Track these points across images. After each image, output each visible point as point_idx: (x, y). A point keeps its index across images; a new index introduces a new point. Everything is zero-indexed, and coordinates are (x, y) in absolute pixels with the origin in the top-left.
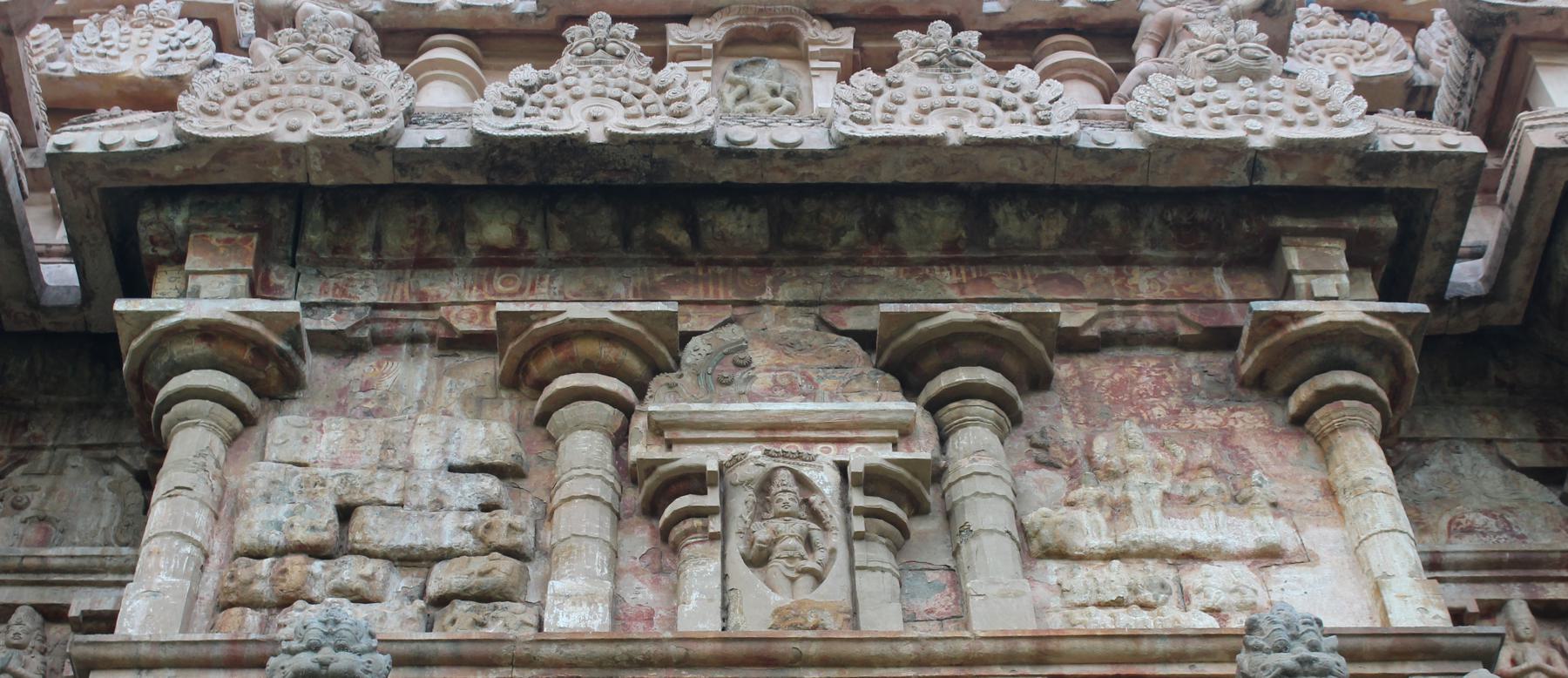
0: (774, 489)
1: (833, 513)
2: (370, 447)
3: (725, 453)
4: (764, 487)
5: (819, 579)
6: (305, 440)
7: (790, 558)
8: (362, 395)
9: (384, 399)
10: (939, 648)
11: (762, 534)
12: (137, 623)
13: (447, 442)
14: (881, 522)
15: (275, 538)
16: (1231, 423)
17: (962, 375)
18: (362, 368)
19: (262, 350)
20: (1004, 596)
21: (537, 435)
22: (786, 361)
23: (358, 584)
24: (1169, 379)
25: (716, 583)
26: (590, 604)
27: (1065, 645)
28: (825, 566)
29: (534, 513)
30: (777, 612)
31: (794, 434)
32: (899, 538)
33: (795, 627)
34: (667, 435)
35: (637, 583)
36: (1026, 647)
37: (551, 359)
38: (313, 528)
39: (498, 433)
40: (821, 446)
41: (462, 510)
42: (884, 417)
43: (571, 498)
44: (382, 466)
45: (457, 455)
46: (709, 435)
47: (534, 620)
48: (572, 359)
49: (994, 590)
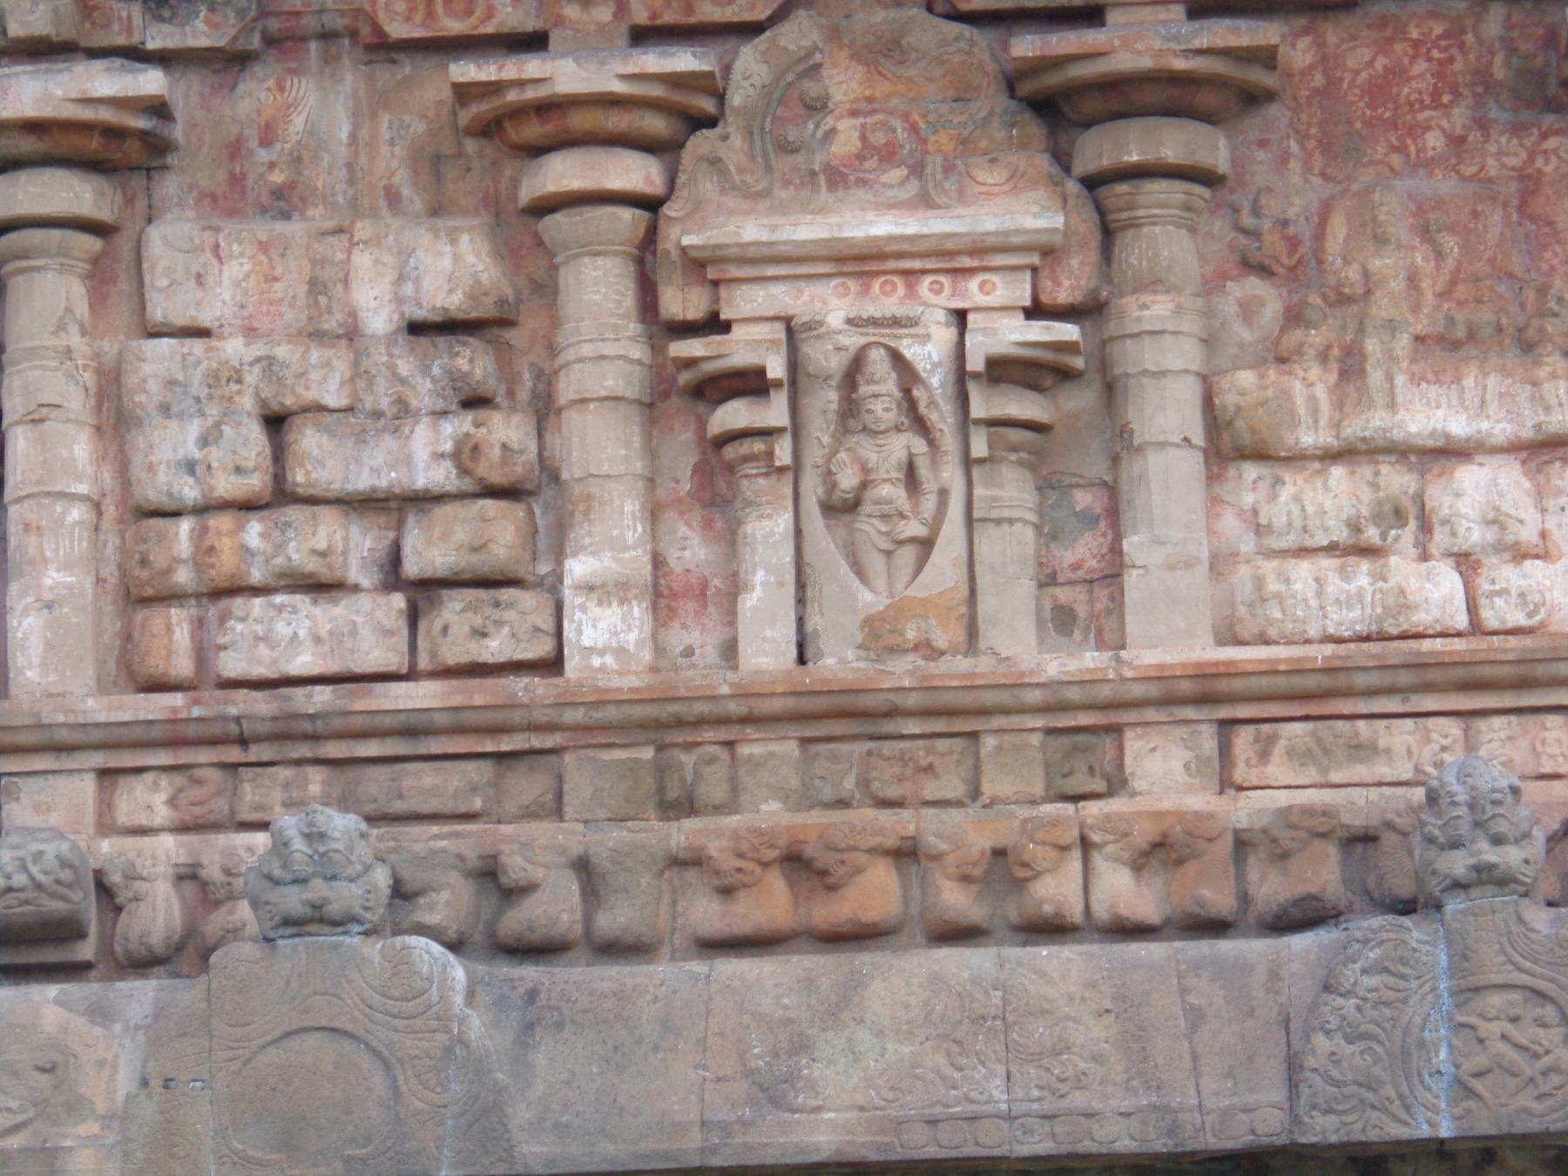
1: (943, 418)
2: (292, 282)
5: (926, 545)
6: (200, 279)
7: (885, 517)
8: (263, 155)
9: (296, 160)
10: (1073, 694)
11: (848, 480)
12: (36, 660)
14: (1015, 435)
15: (189, 492)
16: (1539, 162)
18: (255, 93)
19: (113, 133)
20: (1171, 568)
22: (882, 88)
23: (312, 565)
24: (1458, 66)
25: (787, 556)
27: (1238, 685)
34: (712, 273)
35: (683, 530)
38: (238, 470)
39: (471, 259)
40: (928, 279)
41: (434, 413)
42: (1016, 240)
43: (584, 401)
44: (318, 336)
45: (419, 305)
46: (771, 271)
47: (547, 624)
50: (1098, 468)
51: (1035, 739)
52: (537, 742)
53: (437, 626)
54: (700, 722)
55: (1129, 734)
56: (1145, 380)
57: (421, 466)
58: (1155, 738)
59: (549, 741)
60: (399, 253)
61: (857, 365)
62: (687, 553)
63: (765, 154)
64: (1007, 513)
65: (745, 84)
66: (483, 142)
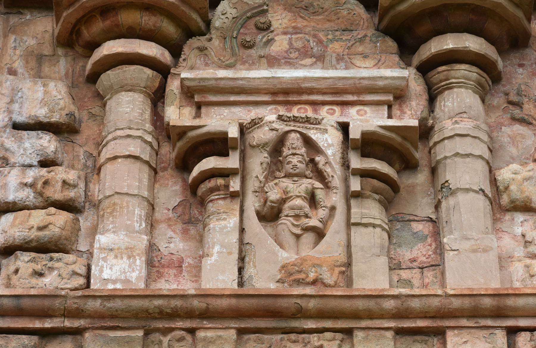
0: (286, 151)
1: (334, 172)
3: (246, 115)
4: (277, 148)
5: (319, 234)
7: (297, 217)
10: (415, 304)
11: (274, 195)
13: (12, 101)
14: (375, 182)
17: (449, 42)
20: (474, 251)
21: (86, 91)
22: (301, 23)
25: (235, 237)
26: (129, 258)
27: (521, 302)
28: (325, 222)
29: (85, 166)
30: (283, 267)
31: (305, 97)
32: (390, 193)
33: (299, 282)
34: (197, 98)
35: (170, 233)
36: (487, 302)
37: (99, 26)
39: (54, 93)
40: (327, 108)
41: (23, 166)
42: (381, 83)
43: (115, 158)
45: (20, 113)
46: (232, 98)
47: (82, 270)
48: (117, 26)
49: (466, 245)
50: (428, 212)
51: (390, 334)
52: (68, 323)
53: (12, 268)
54: (174, 315)
55: (450, 334)
56: (457, 159)
57: (12, 188)
58: (466, 335)
59: (77, 323)
60: (13, 90)
61: (281, 141)
62: (172, 245)
63: (232, 48)
64: (372, 221)
65: (223, 17)
66: (69, 50)
